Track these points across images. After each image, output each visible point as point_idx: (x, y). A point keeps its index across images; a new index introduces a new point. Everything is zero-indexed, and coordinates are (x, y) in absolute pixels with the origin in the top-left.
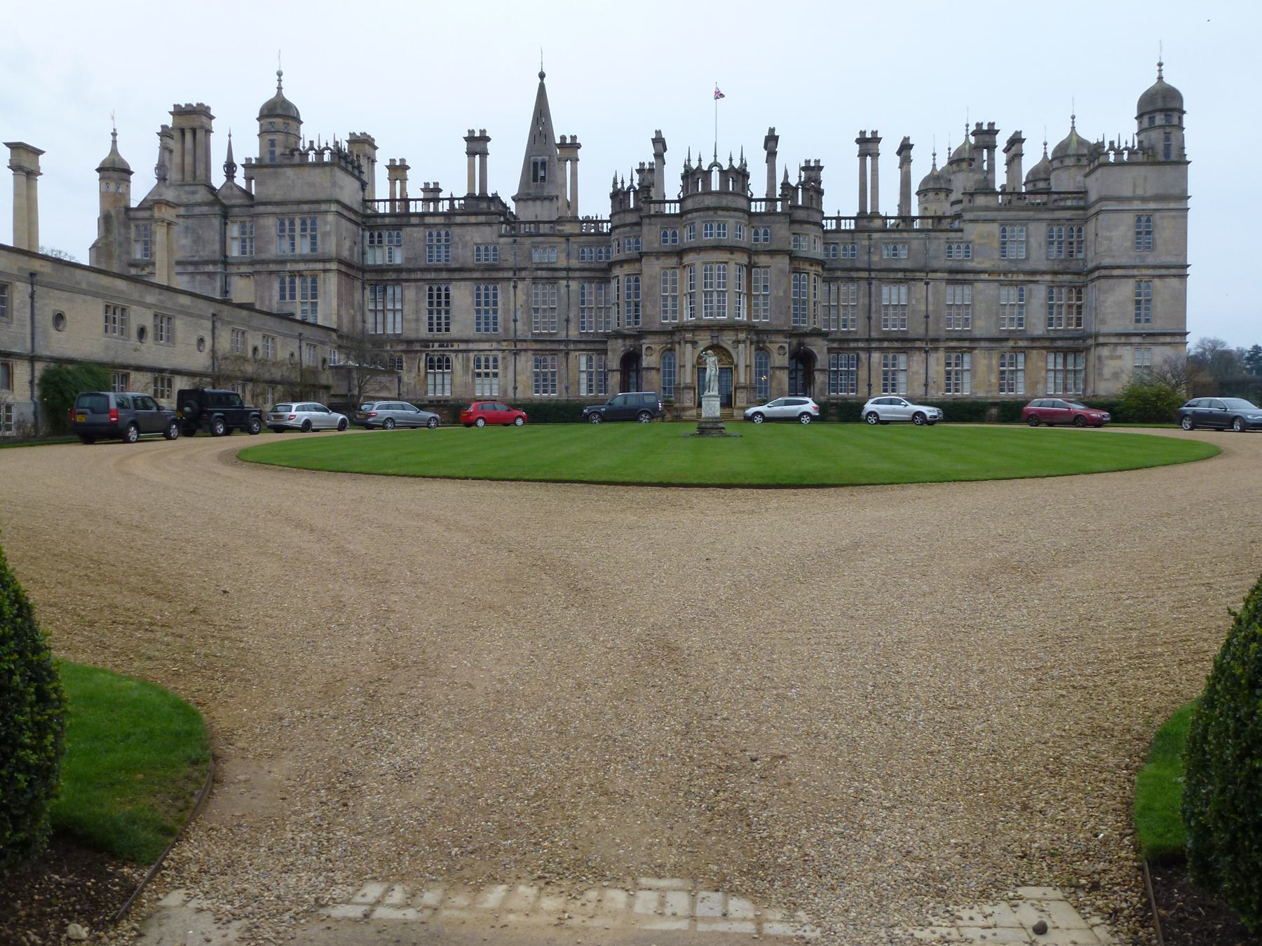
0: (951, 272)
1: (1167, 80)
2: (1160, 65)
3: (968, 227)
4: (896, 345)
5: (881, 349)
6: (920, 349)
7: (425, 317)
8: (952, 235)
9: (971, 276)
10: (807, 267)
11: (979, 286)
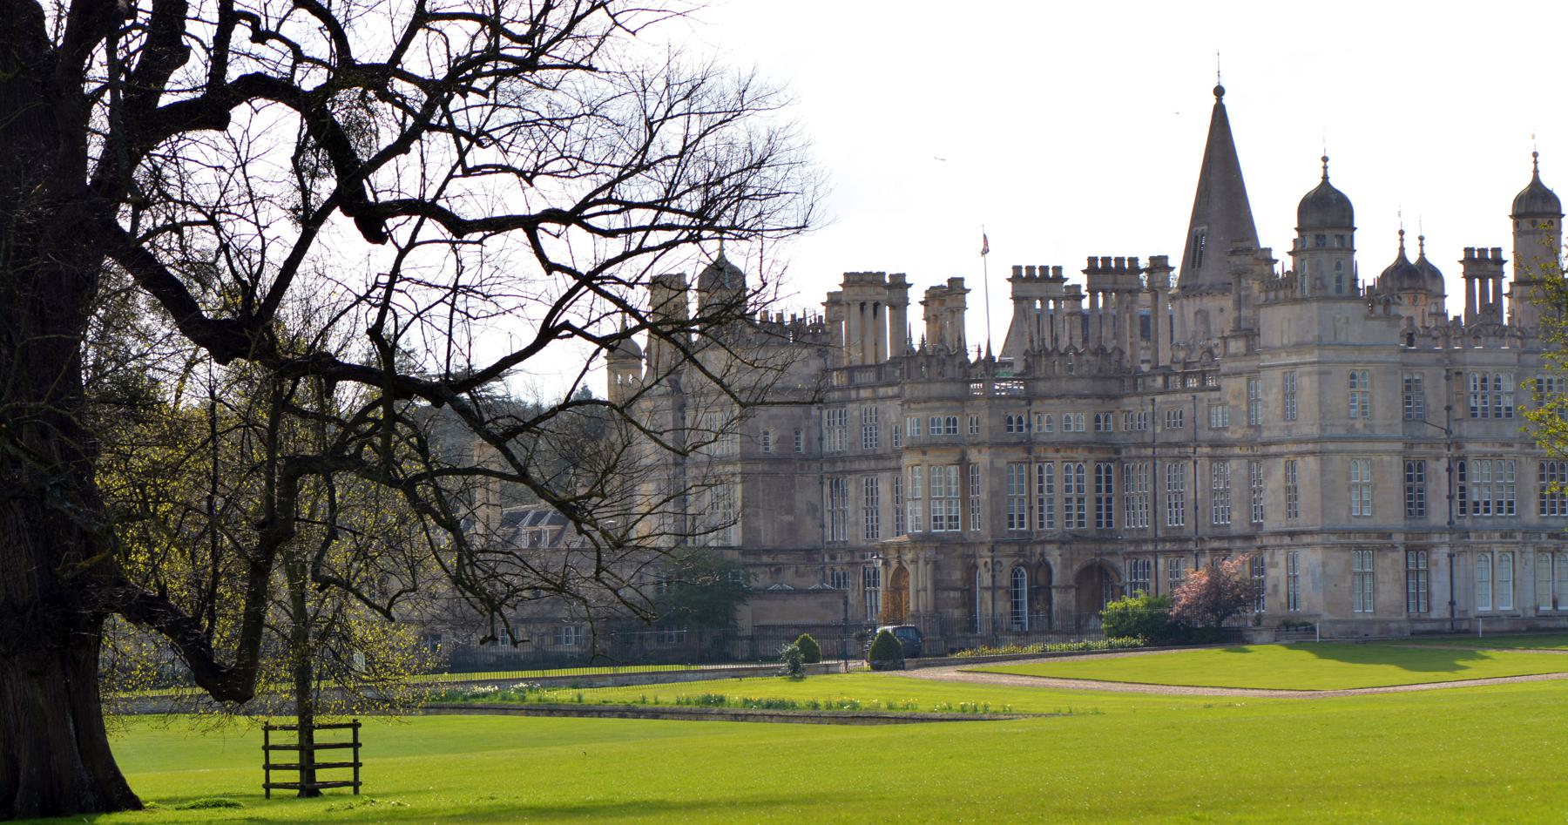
0: (1214, 445)
1: (1332, 181)
2: (1325, 159)
3: (1224, 382)
5: (1163, 552)
6: (1191, 551)
7: (862, 520)
8: (1214, 395)
9: (1227, 451)
10: (1050, 454)
11: (1233, 464)
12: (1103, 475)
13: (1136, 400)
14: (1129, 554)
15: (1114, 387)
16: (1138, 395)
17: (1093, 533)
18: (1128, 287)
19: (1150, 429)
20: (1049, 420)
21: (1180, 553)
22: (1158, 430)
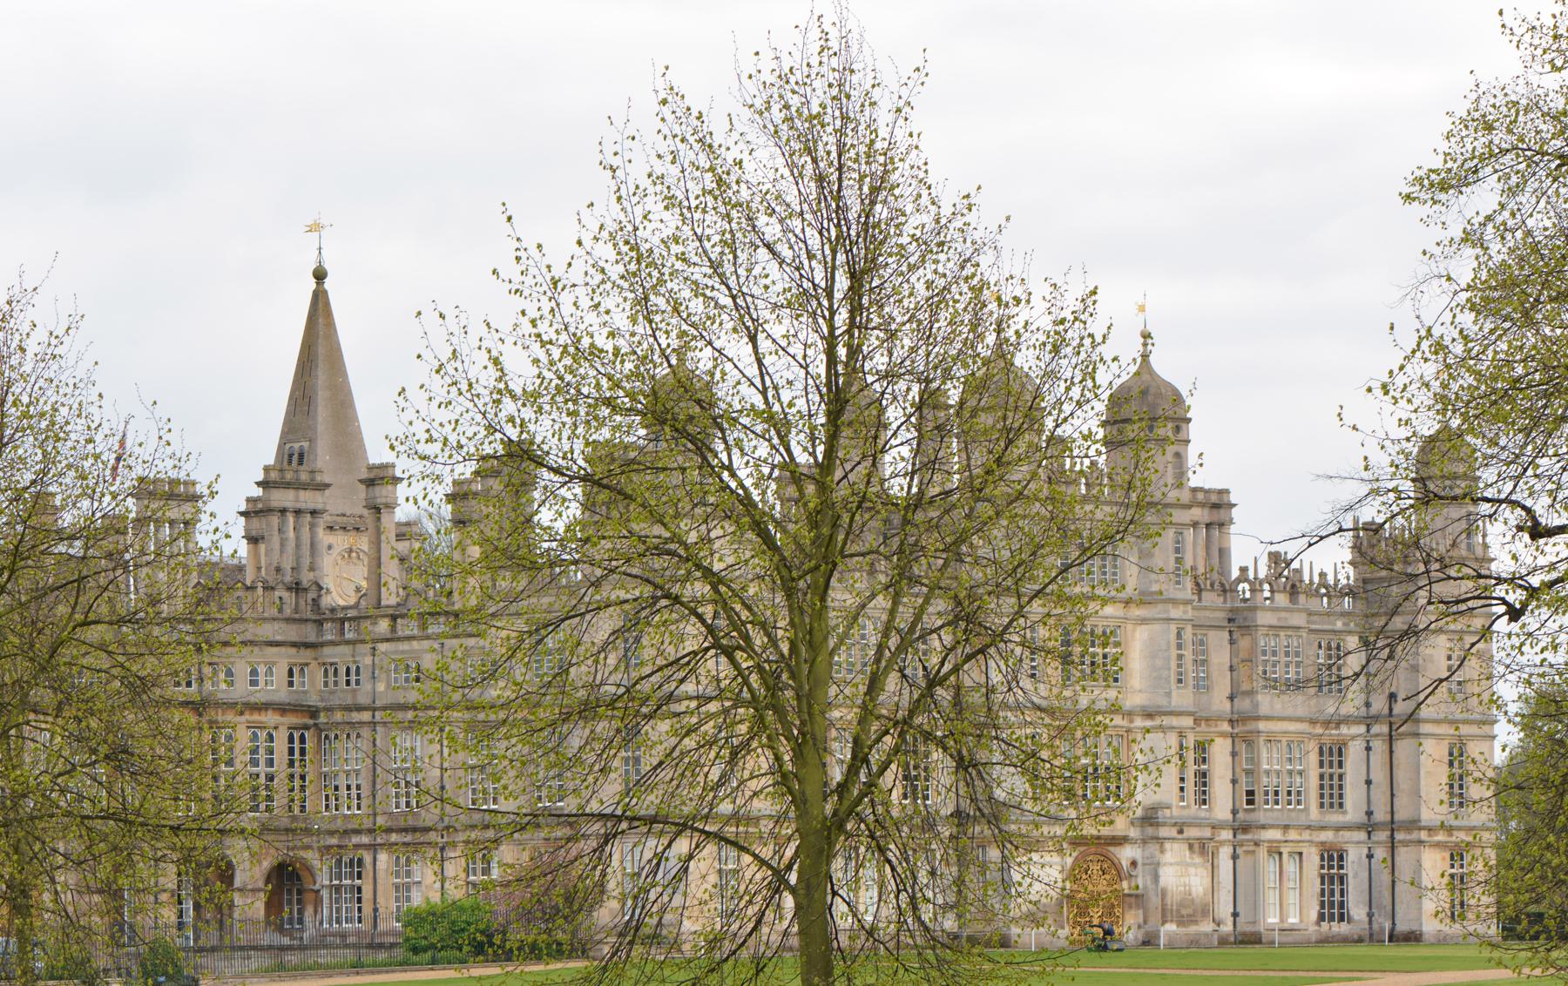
4: (408, 838)
10: (230, 717)
12: (297, 745)
13: (345, 649)
14: (329, 847)
15: (310, 633)
16: (348, 642)
17: (285, 822)
18: (311, 506)
19: (366, 686)
20: (229, 673)
21: (415, 847)
22: (381, 687)
